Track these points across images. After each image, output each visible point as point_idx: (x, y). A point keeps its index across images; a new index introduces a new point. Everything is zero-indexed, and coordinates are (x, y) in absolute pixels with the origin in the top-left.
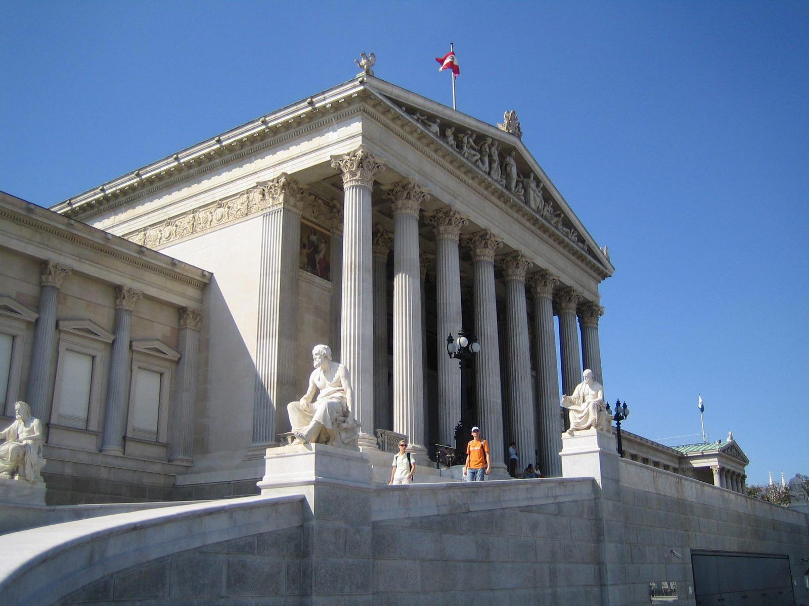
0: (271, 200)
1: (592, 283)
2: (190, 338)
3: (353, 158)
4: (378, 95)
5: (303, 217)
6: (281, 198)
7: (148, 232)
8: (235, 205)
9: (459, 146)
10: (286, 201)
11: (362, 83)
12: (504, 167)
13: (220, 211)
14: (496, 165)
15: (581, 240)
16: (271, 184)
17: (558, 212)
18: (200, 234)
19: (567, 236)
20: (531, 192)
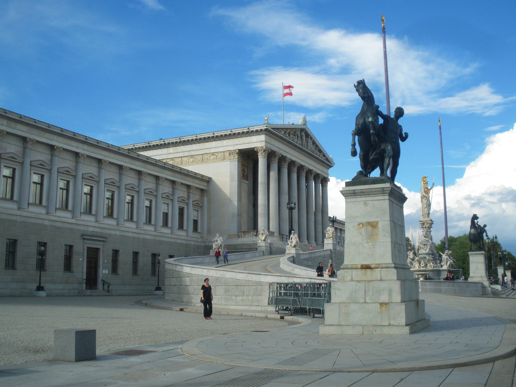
0: (233, 157)
1: (327, 170)
2: (206, 199)
3: (262, 149)
4: (270, 129)
5: (242, 162)
6: (237, 157)
7: (183, 158)
8: (219, 156)
9: (289, 135)
10: (238, 157)
11: (266, 126)
12: (301, 136)
13: (213, 157)
14: (299, 138)
15: (324, 156)
16: (233, 151)
17: (317, 148)
18: (205, 163)
19: (319, 156)
20: (309, 144)
